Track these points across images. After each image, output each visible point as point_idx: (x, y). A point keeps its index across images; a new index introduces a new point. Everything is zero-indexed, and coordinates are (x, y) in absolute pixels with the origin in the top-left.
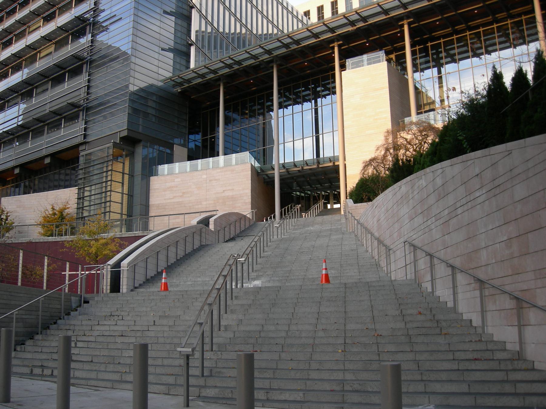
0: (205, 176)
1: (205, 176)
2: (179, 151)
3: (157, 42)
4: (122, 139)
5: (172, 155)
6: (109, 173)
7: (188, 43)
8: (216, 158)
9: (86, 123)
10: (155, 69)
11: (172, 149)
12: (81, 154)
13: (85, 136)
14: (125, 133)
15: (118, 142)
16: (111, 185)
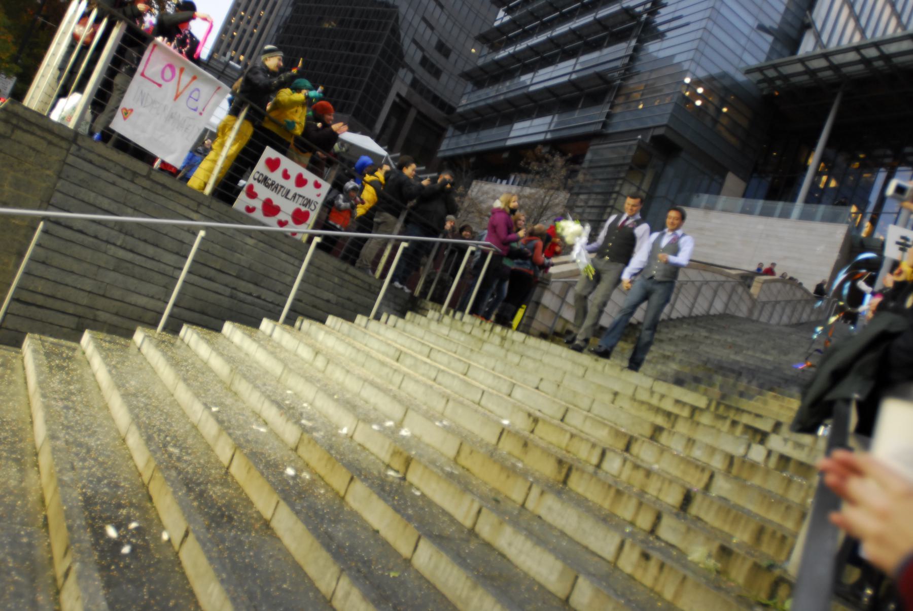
0: (761, 227)
1: (761, 227)
2: (732, 181)
3: (755, 10)
4: (654, 138)
5: (721, 185)
6: (620, 182)
7: (803, 22)
8: (788, 204)
9: (611, 108)
10: (739, 51)
11: (723, 177)
12: (591, 148)
13: (605, 125)
14: (660, 132)
15: (648, 140)
16: (616, 199)
